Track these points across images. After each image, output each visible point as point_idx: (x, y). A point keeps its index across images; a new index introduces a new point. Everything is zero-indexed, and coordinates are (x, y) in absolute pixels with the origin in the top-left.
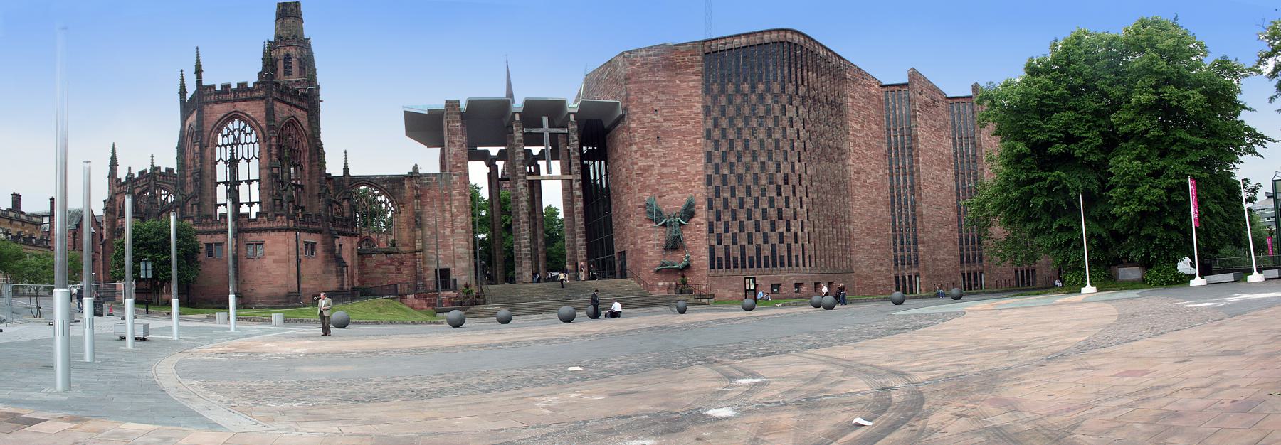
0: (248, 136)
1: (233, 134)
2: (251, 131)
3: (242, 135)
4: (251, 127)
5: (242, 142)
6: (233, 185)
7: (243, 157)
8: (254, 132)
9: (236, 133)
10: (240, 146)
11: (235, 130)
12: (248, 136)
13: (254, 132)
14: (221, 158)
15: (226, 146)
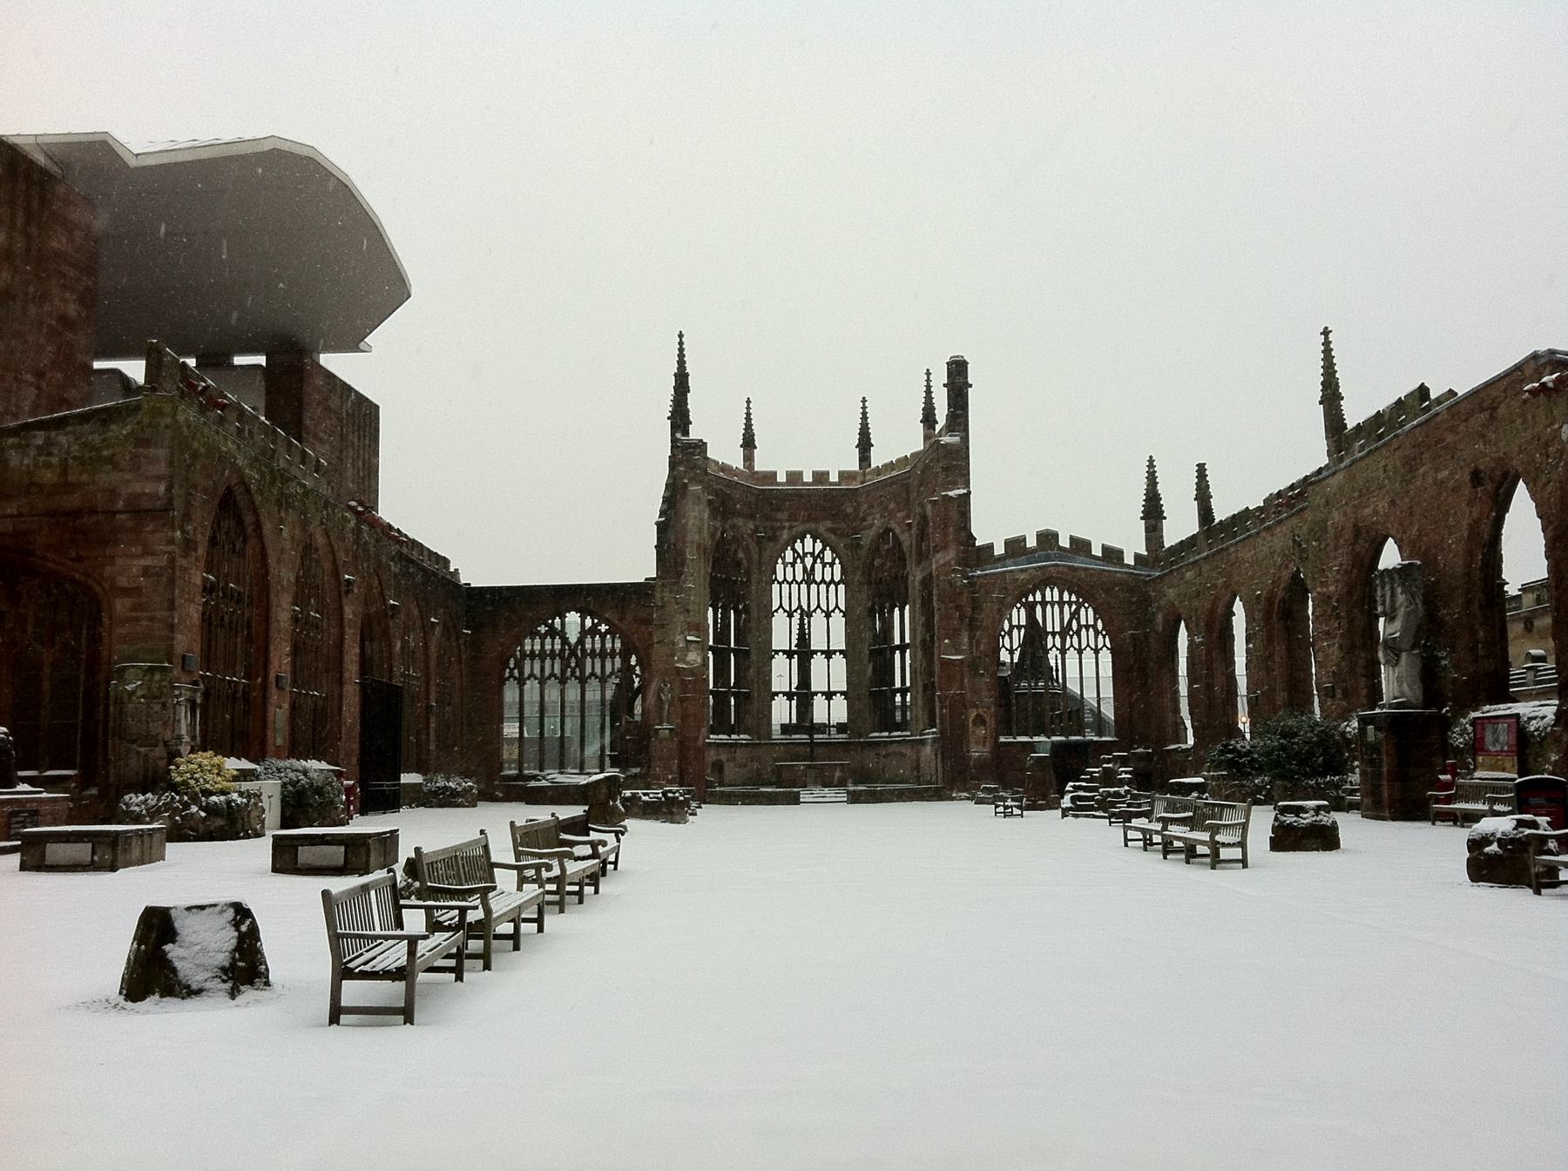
0: (828, 569)
1: (803, 562)
2: (834, 560)
3: (818, 567)
4: (833, 551)
5: (818, 579)
6: (803, 652)
7: (837, 606)
8: (837, 561)
9: (809, 561)
10: (814, 586)
11: (805, 554)
12: (828, 569)
13: (837, 561)
14: (781, 606)
15: (790, 584)
